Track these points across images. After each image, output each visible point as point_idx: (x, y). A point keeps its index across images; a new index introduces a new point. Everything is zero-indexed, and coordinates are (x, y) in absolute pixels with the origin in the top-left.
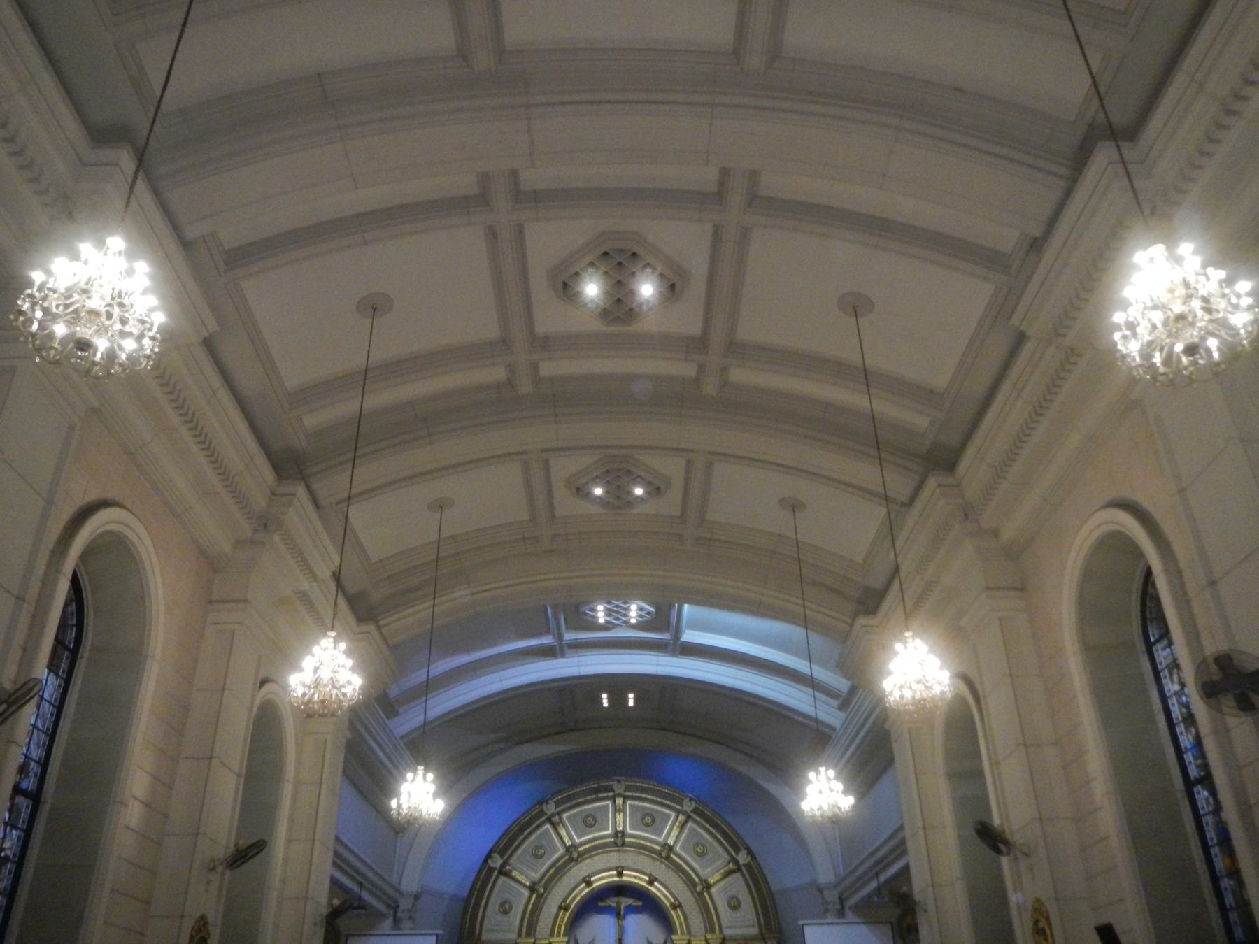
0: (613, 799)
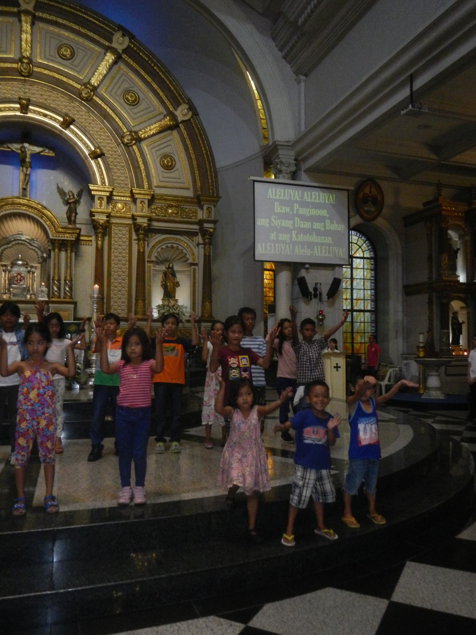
0: (18, 15)
